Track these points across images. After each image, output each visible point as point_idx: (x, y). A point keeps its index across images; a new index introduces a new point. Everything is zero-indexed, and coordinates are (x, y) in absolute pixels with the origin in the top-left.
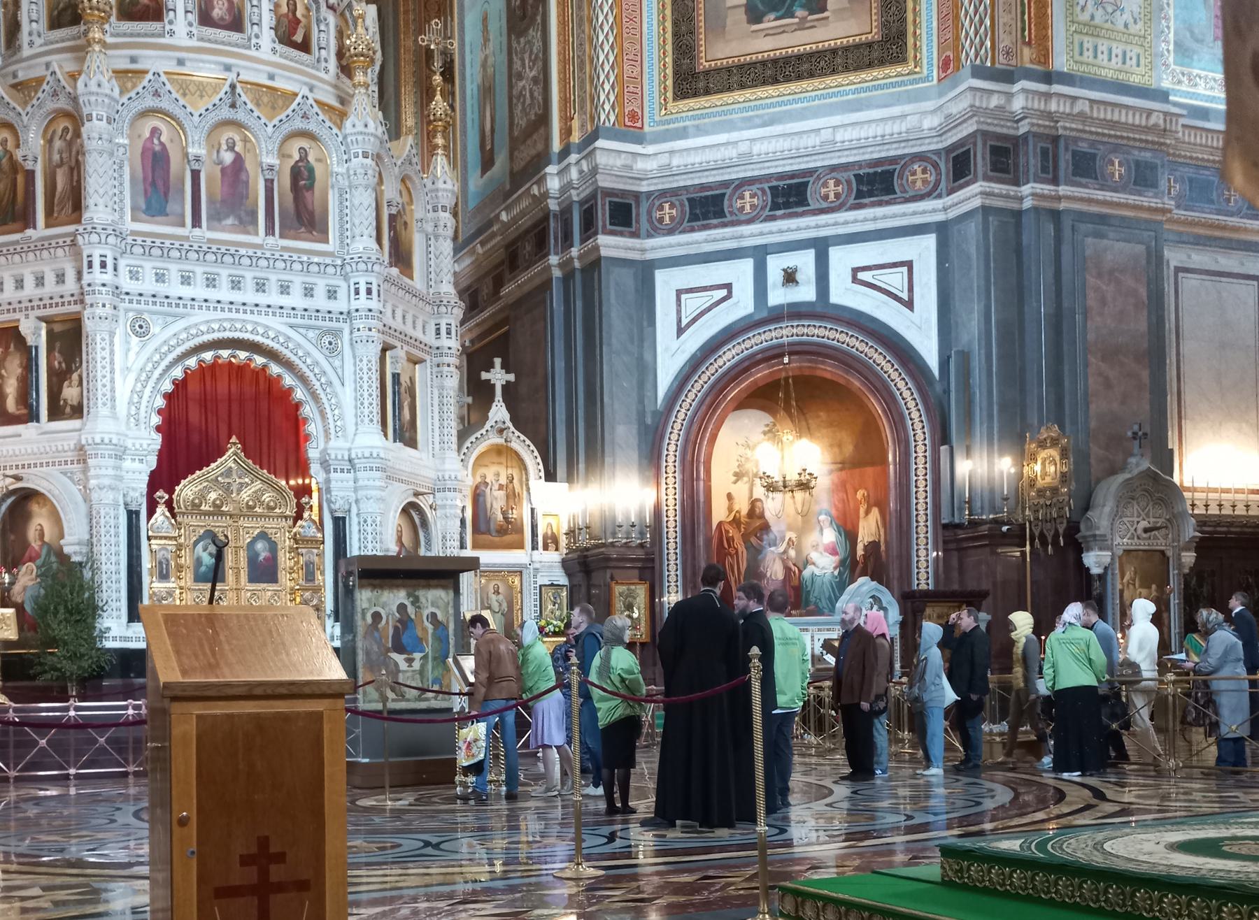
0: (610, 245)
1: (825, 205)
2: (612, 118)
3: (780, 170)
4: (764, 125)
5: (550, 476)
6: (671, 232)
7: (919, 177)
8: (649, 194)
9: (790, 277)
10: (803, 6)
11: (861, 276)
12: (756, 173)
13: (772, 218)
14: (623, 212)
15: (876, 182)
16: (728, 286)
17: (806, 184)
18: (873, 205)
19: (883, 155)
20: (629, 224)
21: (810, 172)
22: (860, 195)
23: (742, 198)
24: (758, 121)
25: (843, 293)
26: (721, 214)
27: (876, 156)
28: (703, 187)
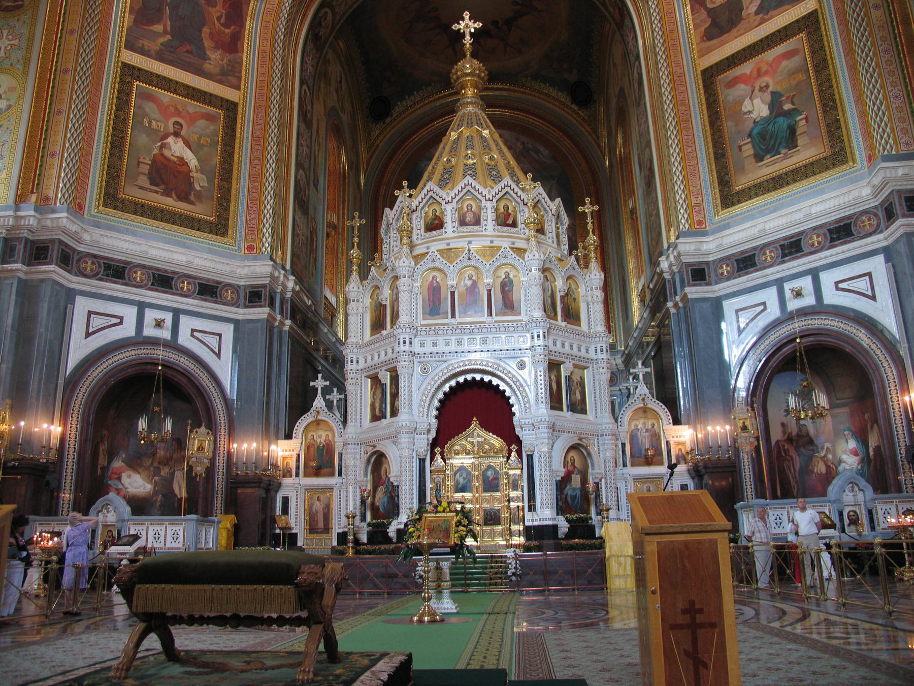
0: (694, 292)
1: (813, 249)
2: (687, 226)
3: (784, 235)
4: (771, 213)
5: (677, 421)
6: (728, 279)
7: (867, 223)
8: (714, 261)
9: (798, 294)
10: (785, 147)
11: (840, 286)
12: (770, 239)
13: (783, 262)
14: (699, 274)
15: (841, 231)
16: (764, 304)
17: (800, 240)
18: (841, 244)
19: (842, 215)
20: (704, 279)
21: (801, 233)
22: (832, 240)
23: (765, 254)
24: (767, 212)
25: (831, 297)
26: (754, 265)
27: (838, 217)
28: (742, 252)
